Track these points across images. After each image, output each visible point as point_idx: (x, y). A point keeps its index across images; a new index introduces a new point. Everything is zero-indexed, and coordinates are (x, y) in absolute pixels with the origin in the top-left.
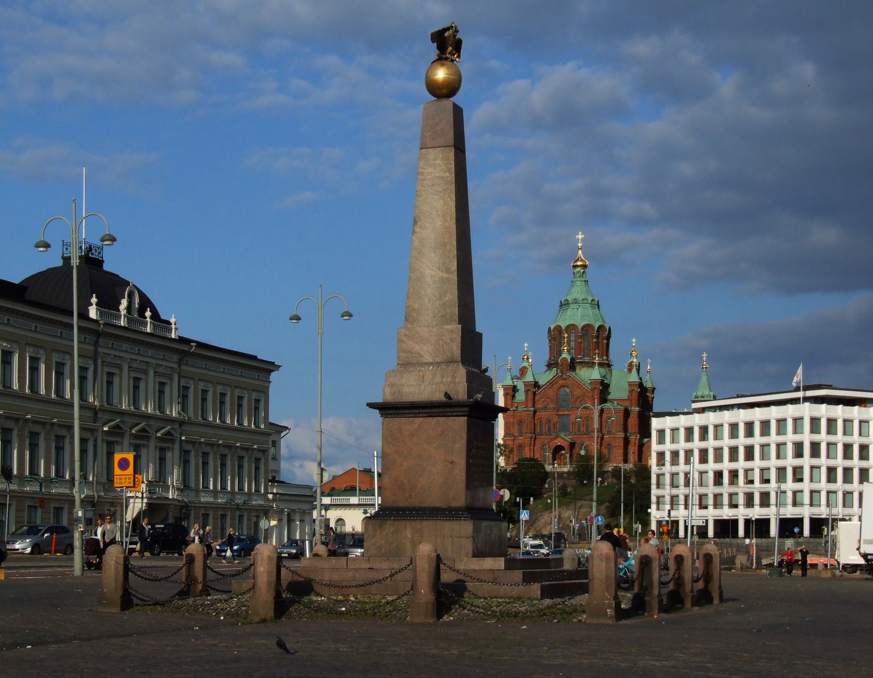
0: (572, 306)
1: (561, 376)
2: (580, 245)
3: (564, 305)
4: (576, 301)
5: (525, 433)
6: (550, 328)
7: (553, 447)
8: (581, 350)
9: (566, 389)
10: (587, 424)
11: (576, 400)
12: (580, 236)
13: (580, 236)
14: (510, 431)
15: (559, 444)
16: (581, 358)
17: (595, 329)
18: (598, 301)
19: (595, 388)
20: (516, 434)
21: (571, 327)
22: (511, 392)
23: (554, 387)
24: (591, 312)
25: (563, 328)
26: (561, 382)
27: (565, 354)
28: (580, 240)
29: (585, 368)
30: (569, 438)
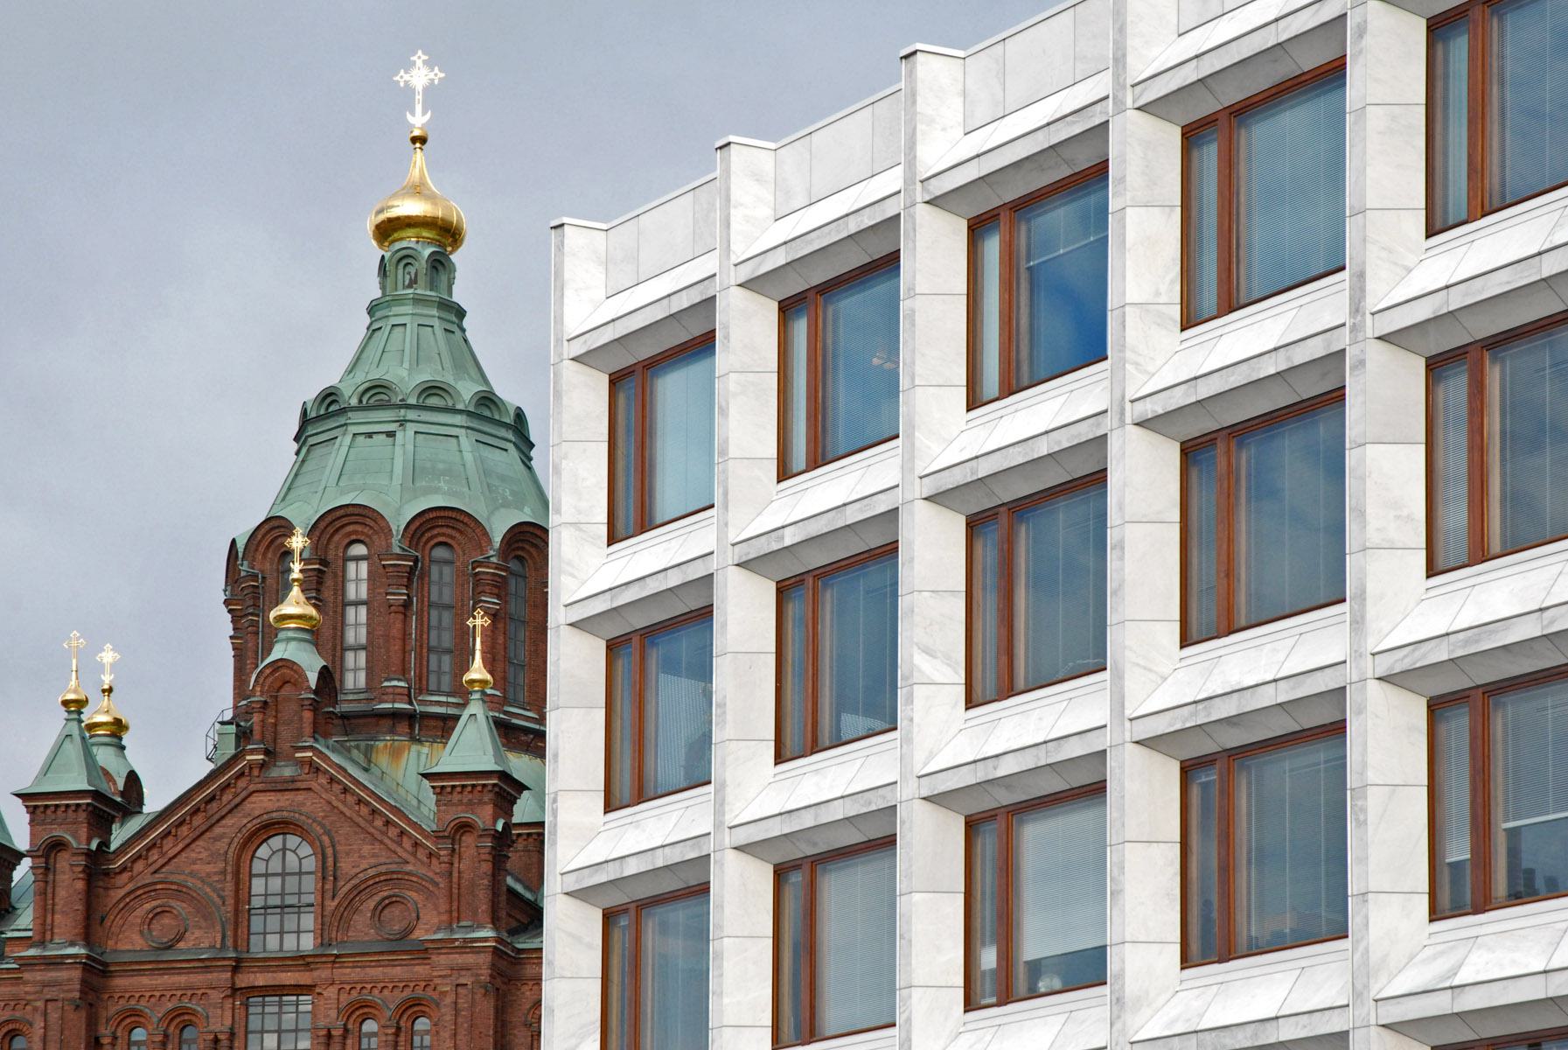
0: (360, 421)
1: (263, 766)
9: (293, 841)
11: (350, 904)
16: (395, 694)
17: (490, 541)
19: (464, 827)
23: (217, 830)
24: (468, 457)
26: (264, 804)
27: (293, 645)
28: (419, 97)
29: (425, 750)
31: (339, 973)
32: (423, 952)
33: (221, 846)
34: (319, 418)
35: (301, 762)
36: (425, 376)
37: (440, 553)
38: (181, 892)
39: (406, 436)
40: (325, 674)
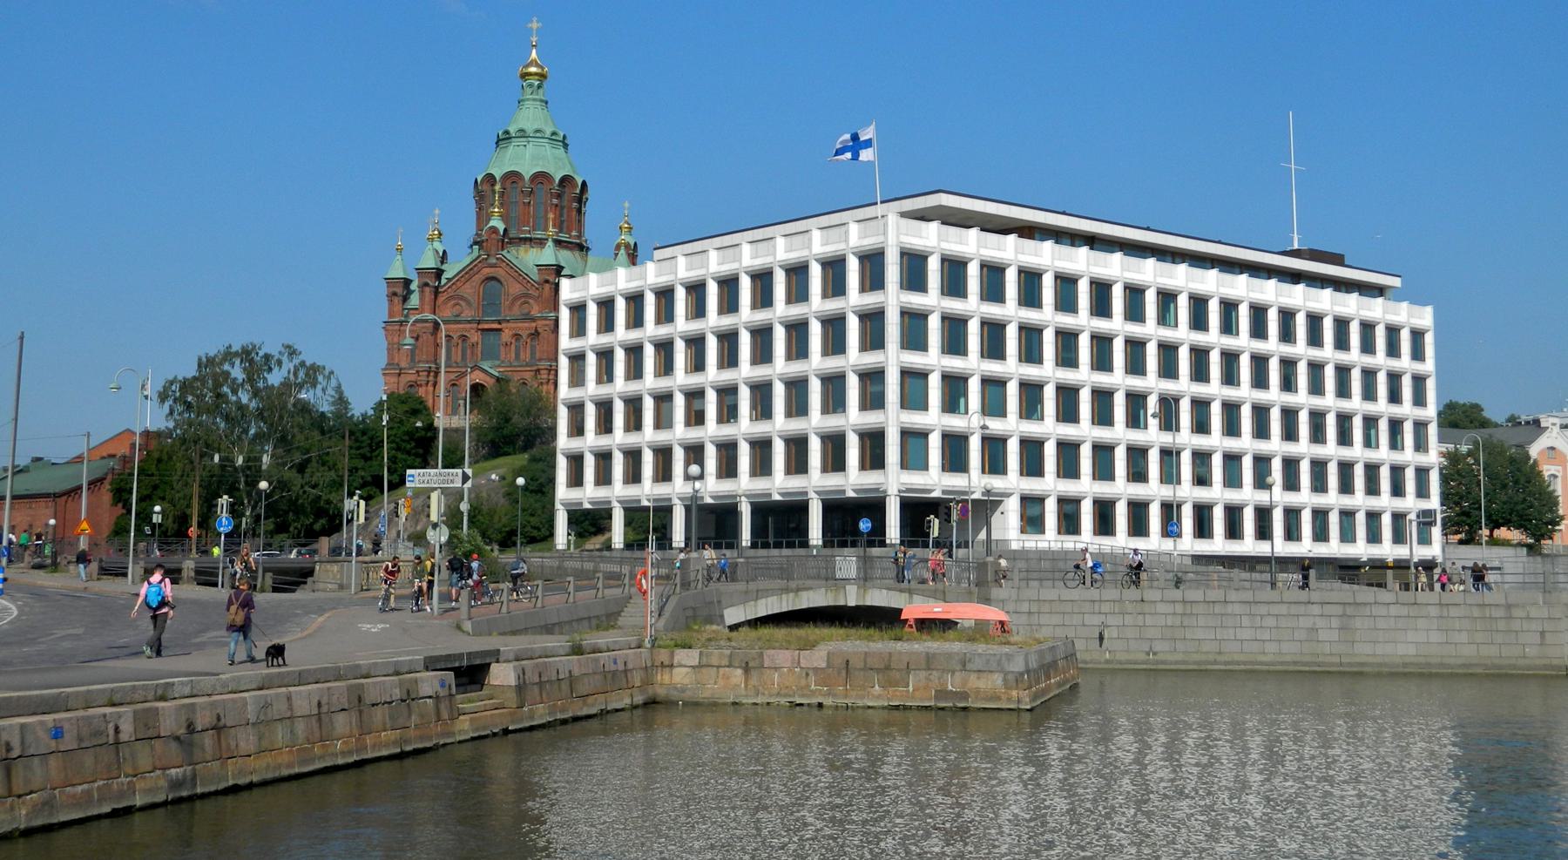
0: (515, 142)
1: (486, 259)
2: (534, 40)
3: (504, 139)
4: (522, 133)
5: (419, 362)
6: (476, 180)
8: (529, 218)
10: (532, 346)
12: (535, 25)
13: (535, 25)
14: (393, 359)
18: (564, 137)
19: (547, 281)
20: (403, 365)
21: (513, 177)
22: (399, 290)
25: (498, 179)
26: (487, 271)
31: (509, 325)
32: (533, 320)
35: (497, 259)
36: (536, 127)
37: (539, 186)
38: (462, 298)
40: (505, 230)
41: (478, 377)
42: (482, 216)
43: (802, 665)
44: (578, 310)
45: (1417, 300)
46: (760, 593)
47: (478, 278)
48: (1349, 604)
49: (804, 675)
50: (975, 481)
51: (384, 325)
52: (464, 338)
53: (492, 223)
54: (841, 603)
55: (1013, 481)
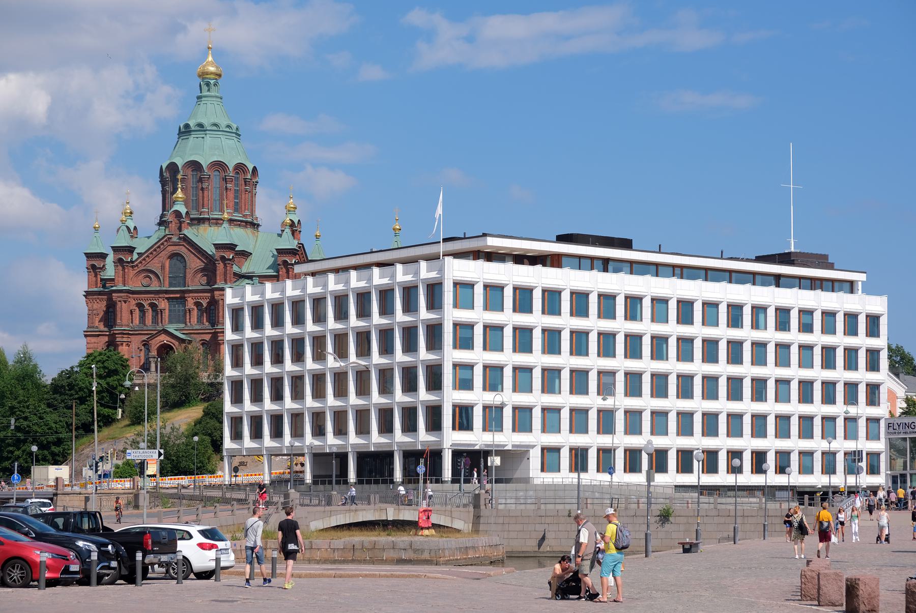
3: (185, 131)
6: (162, 166)
7: (158, 345)
15: (165, 341)
23: (160, 255)
29: (212, 228)
30: (183, 334)
31: (191, 295)
33: (161, 259)
34: (184, 132)
36: (212, 121)
39: (208, 138)
40: (187, 213)
41: (164, 339)
42: (167, 201)
43: (331, 548)
44: (237, 312)
45: (870, 289)
46: (332, 513)
47: (164, 254)
48: (691, 516)
49: (332, 552)
50: (507, 438)
51: (84, 294)
52: (153, 306)
53: (176, 208)
54: (384, 518)
55: (537, 438)
